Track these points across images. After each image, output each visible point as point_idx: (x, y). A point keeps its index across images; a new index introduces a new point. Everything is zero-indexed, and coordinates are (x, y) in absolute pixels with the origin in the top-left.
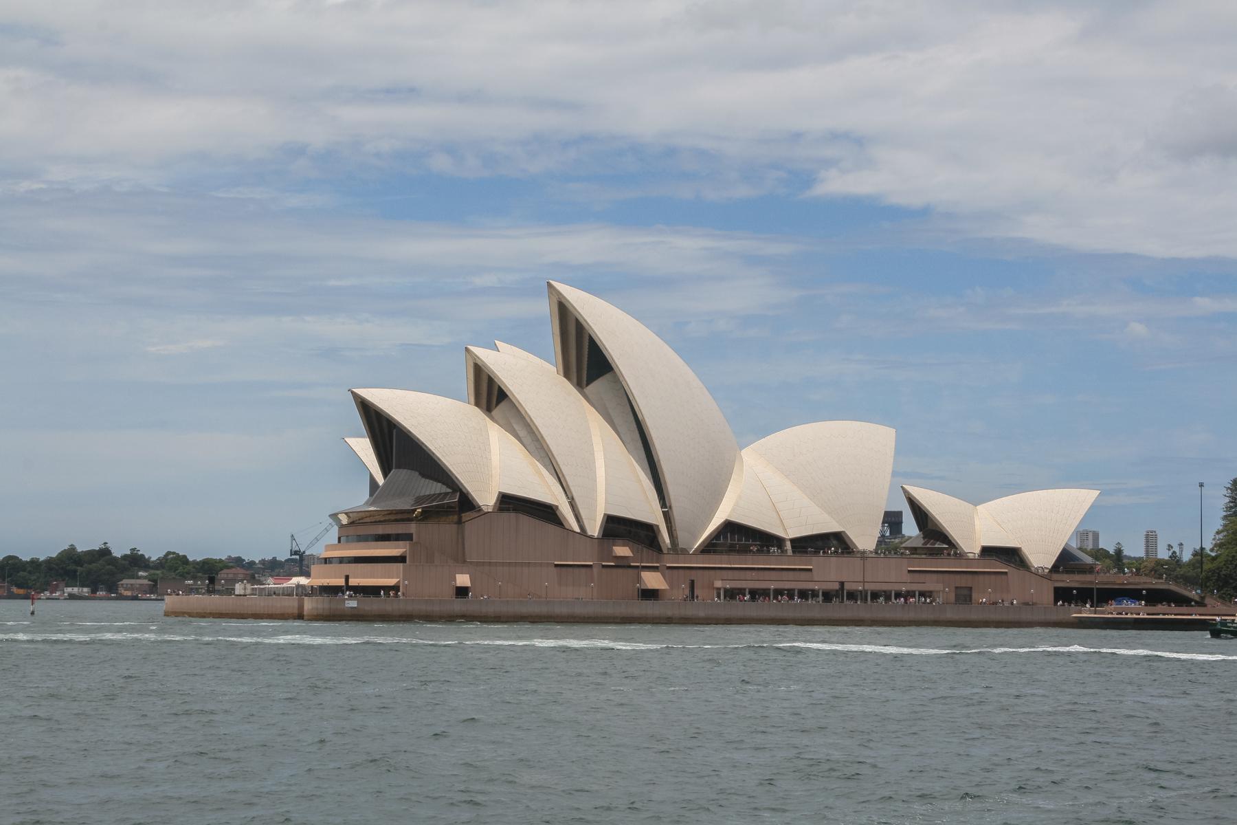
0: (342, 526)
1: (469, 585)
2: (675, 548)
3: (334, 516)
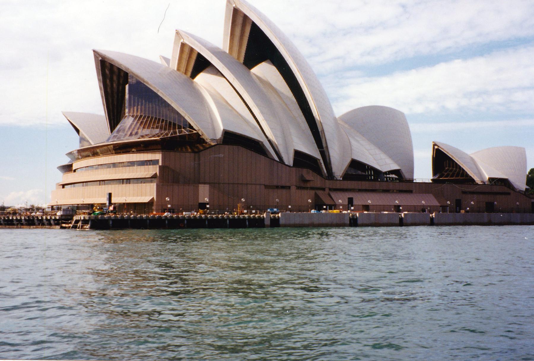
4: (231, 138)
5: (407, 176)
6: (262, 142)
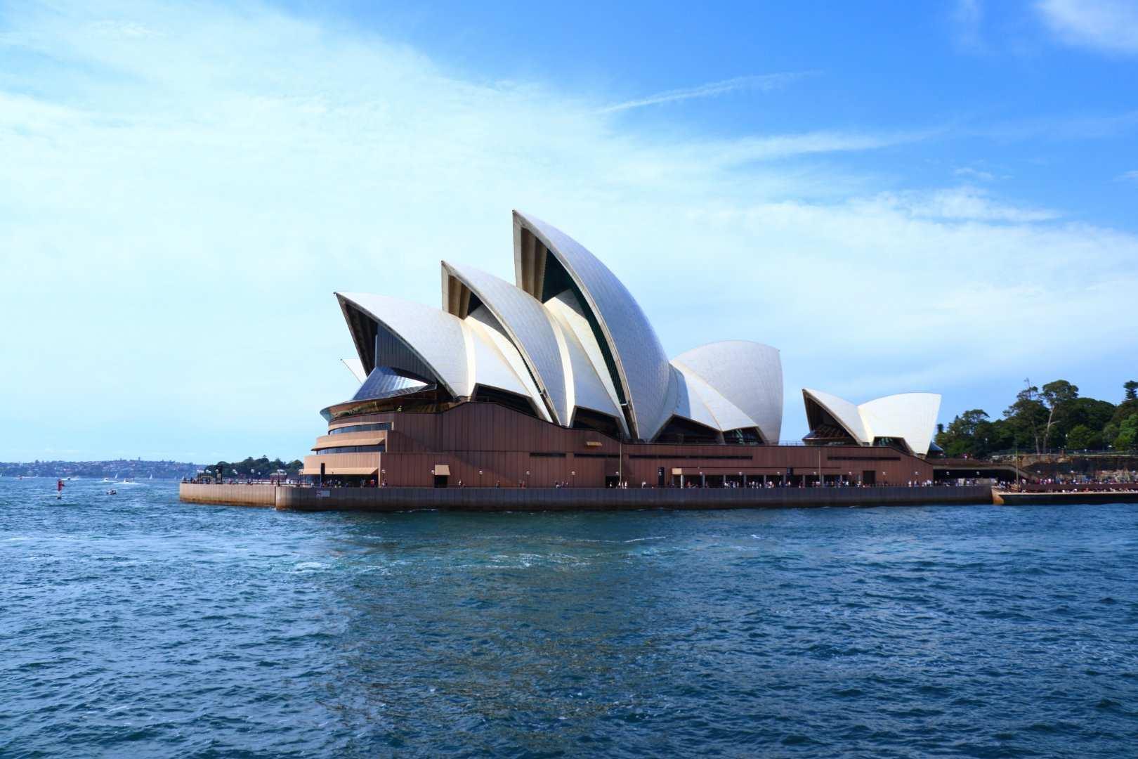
1: (448, 473)
2: (633, 438)
4: (483, 392)
5: (767, 434)
6: (531, 399)
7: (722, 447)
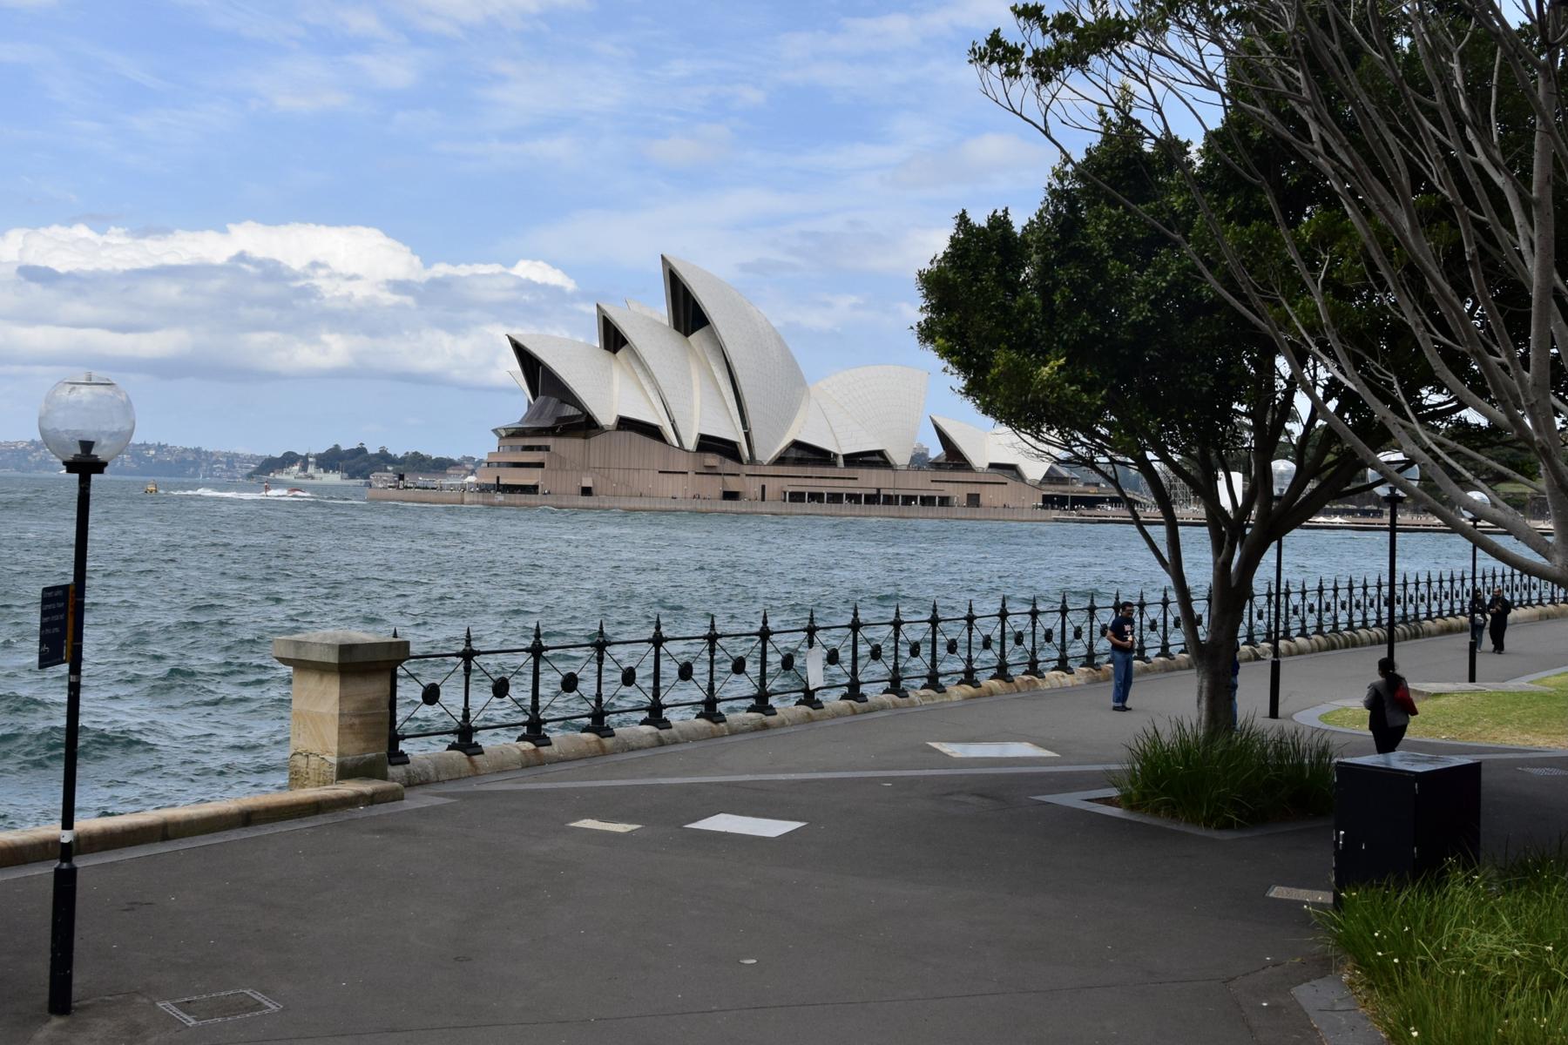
0: (501, 438)
3: (495, 431)
7: (841, 468)
